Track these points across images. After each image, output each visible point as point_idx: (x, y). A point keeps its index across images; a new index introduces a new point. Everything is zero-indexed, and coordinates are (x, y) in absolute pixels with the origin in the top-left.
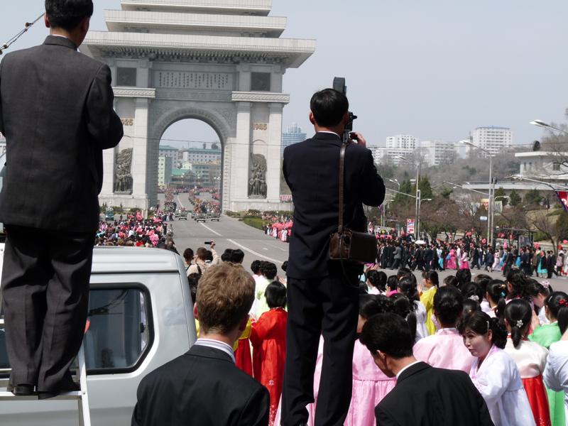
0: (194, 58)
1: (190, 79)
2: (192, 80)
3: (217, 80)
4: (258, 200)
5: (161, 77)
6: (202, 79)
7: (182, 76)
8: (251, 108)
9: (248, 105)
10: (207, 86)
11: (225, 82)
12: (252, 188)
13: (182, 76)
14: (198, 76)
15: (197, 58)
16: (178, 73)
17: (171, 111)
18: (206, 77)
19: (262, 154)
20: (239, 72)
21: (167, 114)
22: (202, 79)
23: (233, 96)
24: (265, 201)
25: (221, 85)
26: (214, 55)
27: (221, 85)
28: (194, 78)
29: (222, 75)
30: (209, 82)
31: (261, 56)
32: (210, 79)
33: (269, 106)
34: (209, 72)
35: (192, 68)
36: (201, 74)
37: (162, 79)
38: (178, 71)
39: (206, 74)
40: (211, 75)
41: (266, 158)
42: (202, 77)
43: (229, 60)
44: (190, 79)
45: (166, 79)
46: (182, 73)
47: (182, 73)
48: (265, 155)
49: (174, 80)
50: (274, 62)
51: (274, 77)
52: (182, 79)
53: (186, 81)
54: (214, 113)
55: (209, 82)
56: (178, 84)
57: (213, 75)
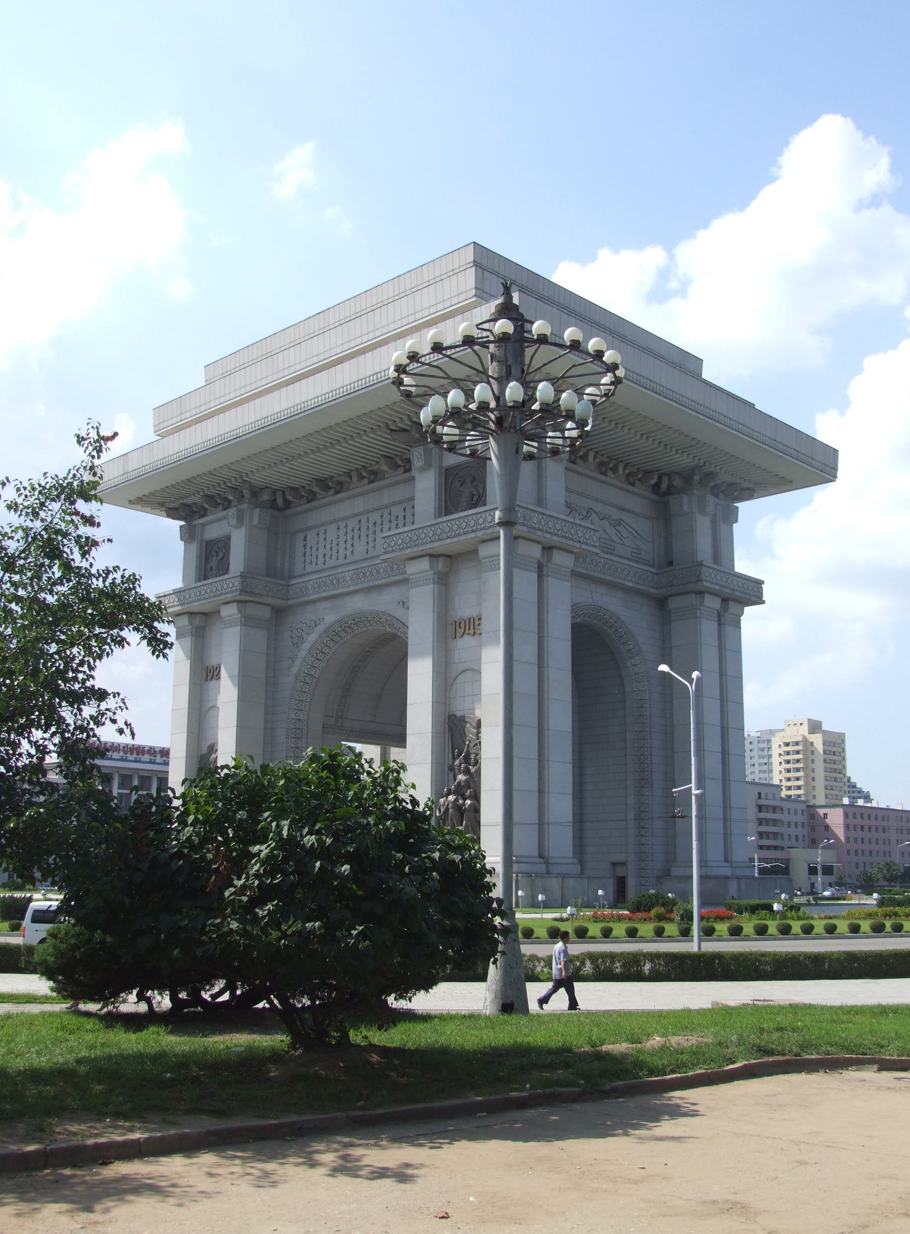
0: (355, 478)
1: (356, 533)
2: (359, 537)
5: (305, 546)
6: (378, 528)
7: (342, 530)
13: (342, 530)
15: (362, 478)
16: (334, 526)
17: (320, 629)
21: (312, 637)
28: (364, 532)
35: (359, 505)
37: (308, 550)
38: (335, 521)
44: (356, 533)
45: (314, 548)
46: (342, 525)
49: (328, 547)
52: (342, 538)
53: (349, 543)
56: (334, 556)
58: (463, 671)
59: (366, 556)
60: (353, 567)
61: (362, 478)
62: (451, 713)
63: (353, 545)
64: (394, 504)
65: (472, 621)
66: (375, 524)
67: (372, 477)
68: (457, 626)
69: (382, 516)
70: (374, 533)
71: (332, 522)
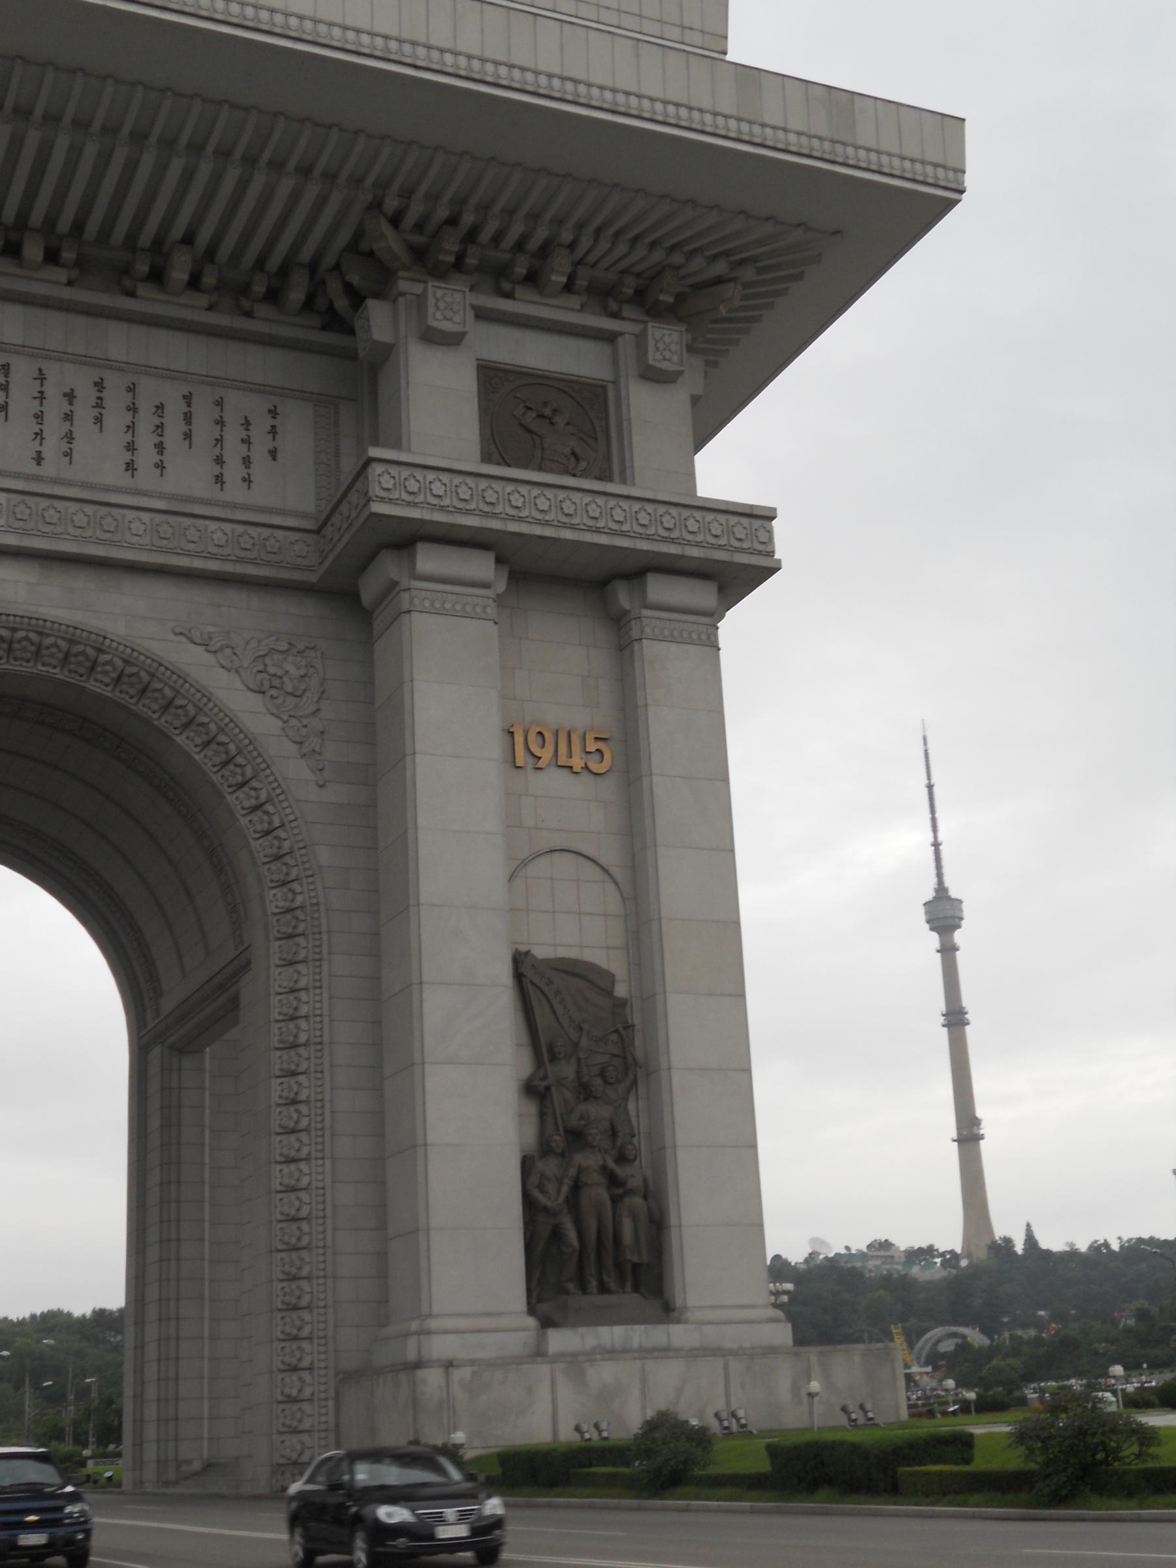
0: (33, 250)
3: (203, 428)
4: (639, 1335)
6: (84, 412)
8: (499, 600)
9: (481, 566)
10: (130, 467)
11: (259, 453)
12: (557, 1234)
14: (51, 390)
15: (52, 257)
18: (116, 398)
19: (598, 958)
20: (385, 355)
22: (84, 412)
23: (381, 479)
24: (678, 1334)
25: (233, 471)
26: (188, 239)
27: (233, 471)
29: (233, 398)
30: (146, 441)
31: (545, 251)
32: (146, 421)
33: (623, 597)
34: (148, 370)
36: (81, 380)
39: (115, 384)
40: (150, 390)
41: (621, 991)
42: (86, 395)
43: (296, 295)
50: (628, 311)
55: (146, 441)
57: (172, 396)
58: (551, 851)
59: (31, 468)
60: (20, 485)
61: (52, 257)
62: (523, 948)
64: (148, 370)
65: (576, 739)
66: (70, 396)
67: (75, 273)
68: (532, 737)
69: (99, 385)
70: (69, 417)
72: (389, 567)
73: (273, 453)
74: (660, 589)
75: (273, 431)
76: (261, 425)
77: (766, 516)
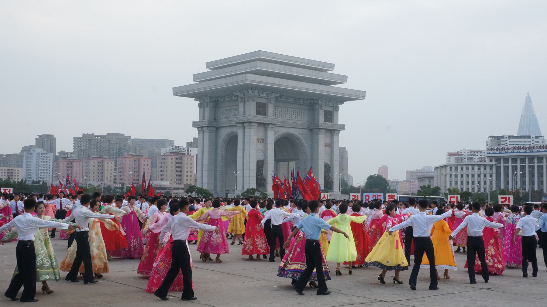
3: (300, 115)
9: (324, 131)
10: (296, 118)
11: (304, 115)
14: (291, 112)
18: (295, 112)
24: (334, 193)
27: (302, 118)
33: (333, 132)
42: (293, 112)
47: (283, 108)
48: (329, 163)
51: (335, 113)
54: (300, 136)
56: (281, 116)
63: (286, 115)
71: (280, 106)
72: (318, 130)
73: (305, 116)
74: (336, 132)
75: (305, 113)
76: (304, 113)
77: (344, 125)
